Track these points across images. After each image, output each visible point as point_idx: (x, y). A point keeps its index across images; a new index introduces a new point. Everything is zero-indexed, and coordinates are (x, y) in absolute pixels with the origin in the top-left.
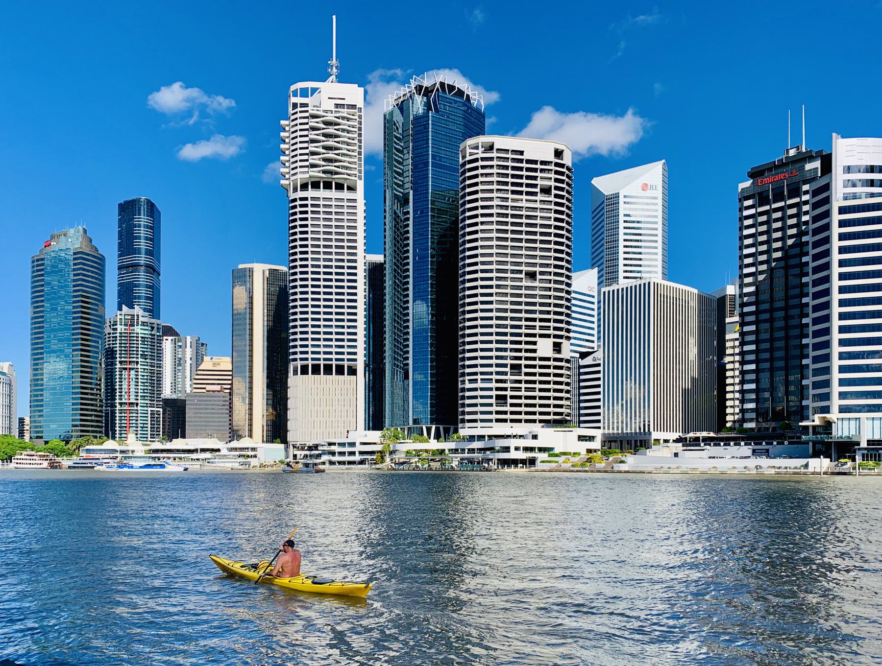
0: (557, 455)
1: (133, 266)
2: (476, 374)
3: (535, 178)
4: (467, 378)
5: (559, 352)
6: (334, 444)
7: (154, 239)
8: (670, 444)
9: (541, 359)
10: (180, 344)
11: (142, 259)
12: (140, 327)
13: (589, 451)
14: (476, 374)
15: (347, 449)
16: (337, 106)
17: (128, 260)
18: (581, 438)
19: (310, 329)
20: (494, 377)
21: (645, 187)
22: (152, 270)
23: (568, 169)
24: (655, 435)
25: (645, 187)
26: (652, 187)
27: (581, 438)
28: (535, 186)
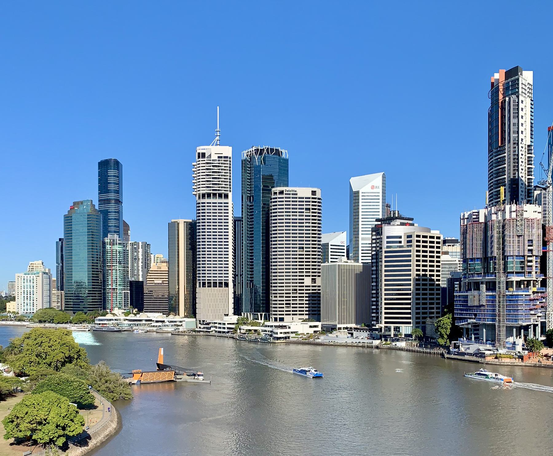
0: (299, 335)
1: (107, 200)
2: (276, 294)
3: (303, 205)
4: (273, 295)
5: (315, 283)
6: (216, 323)
7: (119, 184)
8: (342, 330)
9: (306, 286)
10: (135, 246)
11: (112, 196)
12: (118, 246)
13: (315, 332)
14: (276, 294)
15: (222, 326)
16: (219, 157)
17: (104, 196)
18: (311, 327)
19: (206, 240)
20: (285, 295)
21: (373, 187)
22: (118, 202)
23: (319, 199)
24: (339, 326)
25: (373, 187)
26: (376, 187)
27: (311, 327)
28: (303, 209)
